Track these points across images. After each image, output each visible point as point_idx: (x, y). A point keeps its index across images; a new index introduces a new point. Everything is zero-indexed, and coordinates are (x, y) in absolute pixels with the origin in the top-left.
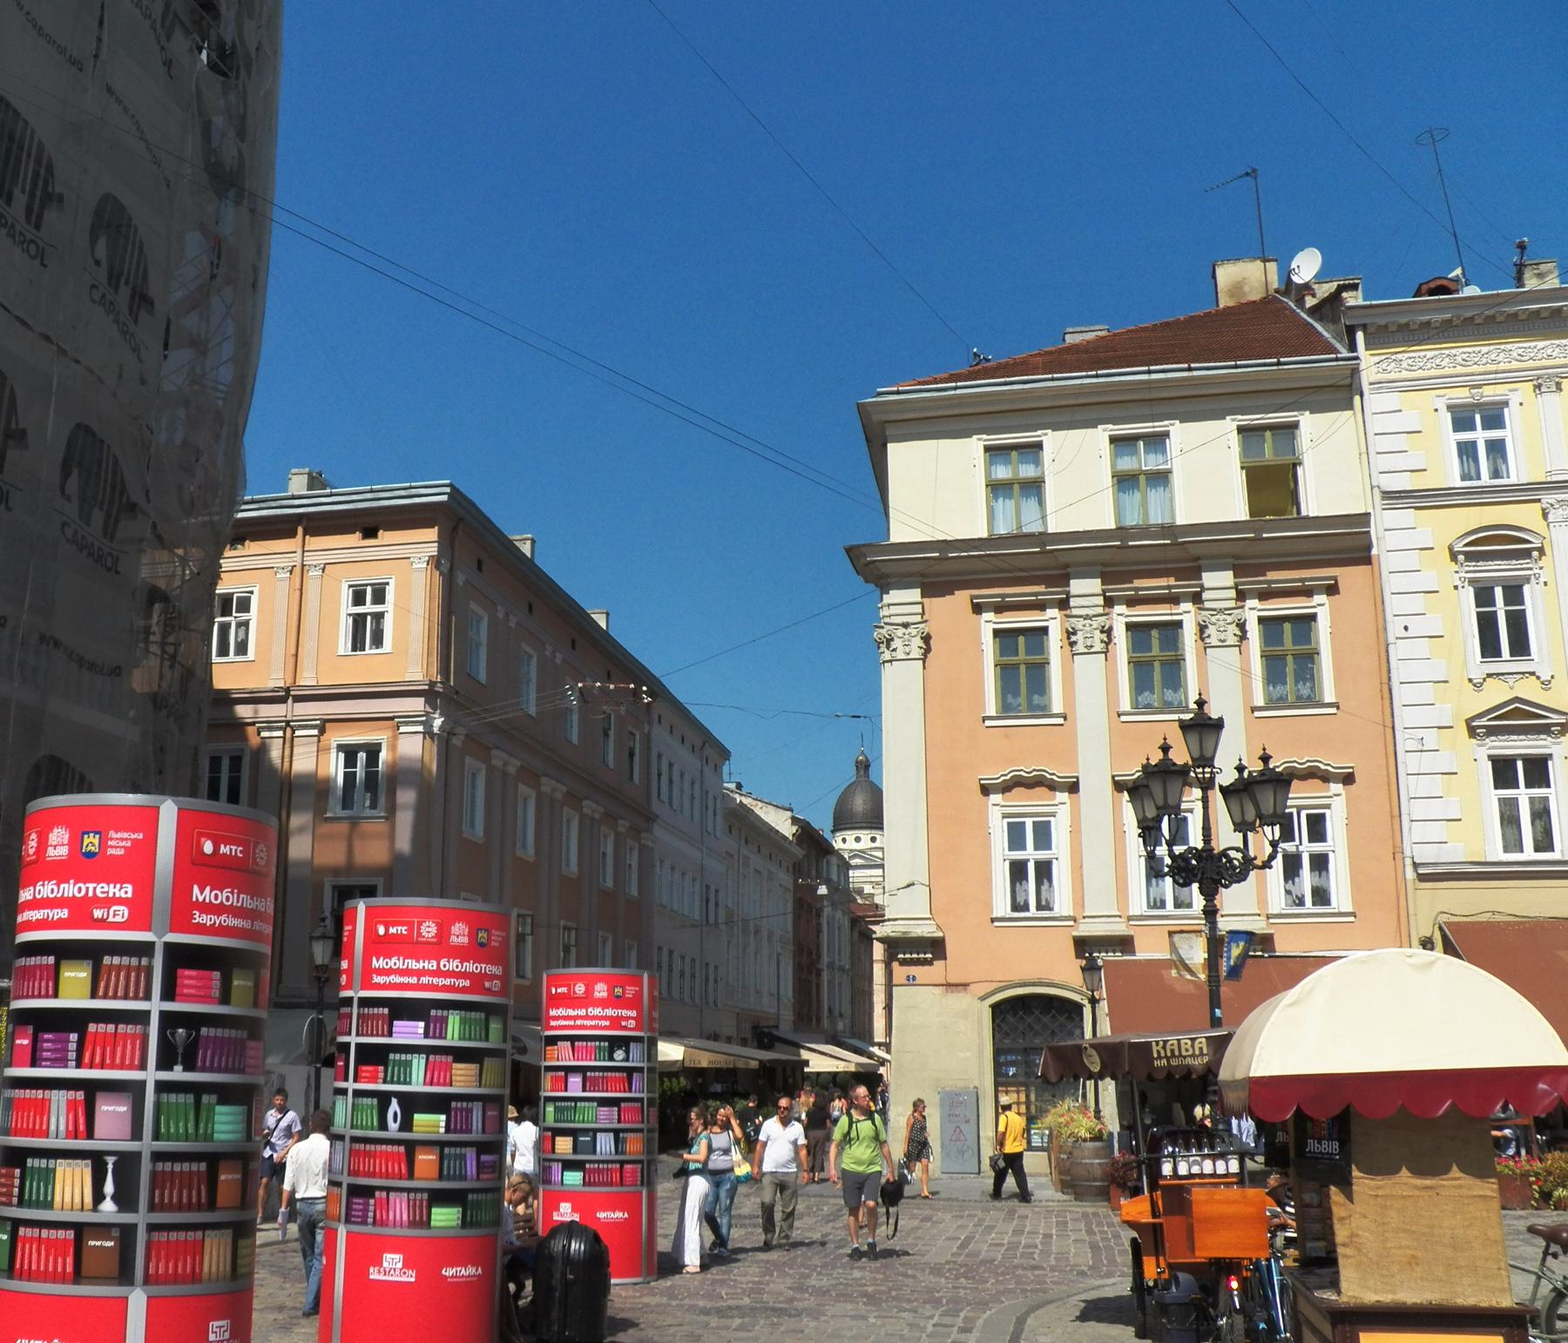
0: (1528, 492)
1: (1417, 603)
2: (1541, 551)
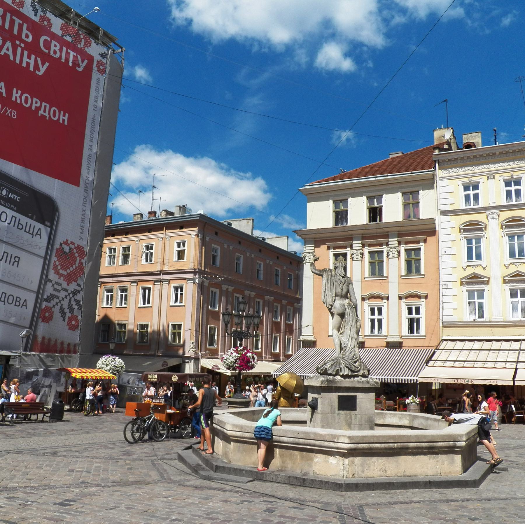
0: (483, 210)
1: (450, 244)
2: (485, 228)
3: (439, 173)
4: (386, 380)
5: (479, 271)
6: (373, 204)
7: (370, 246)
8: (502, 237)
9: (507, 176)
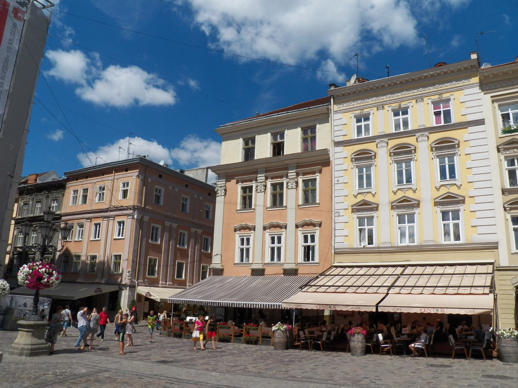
1: (342, 173)
2: (375, 156)
3: (334, 107)
4: (265, 305)
5: (369, 198)
6: (277, 140)
7: (272, 178)
8: (391, 163)
9: (395, 106)
